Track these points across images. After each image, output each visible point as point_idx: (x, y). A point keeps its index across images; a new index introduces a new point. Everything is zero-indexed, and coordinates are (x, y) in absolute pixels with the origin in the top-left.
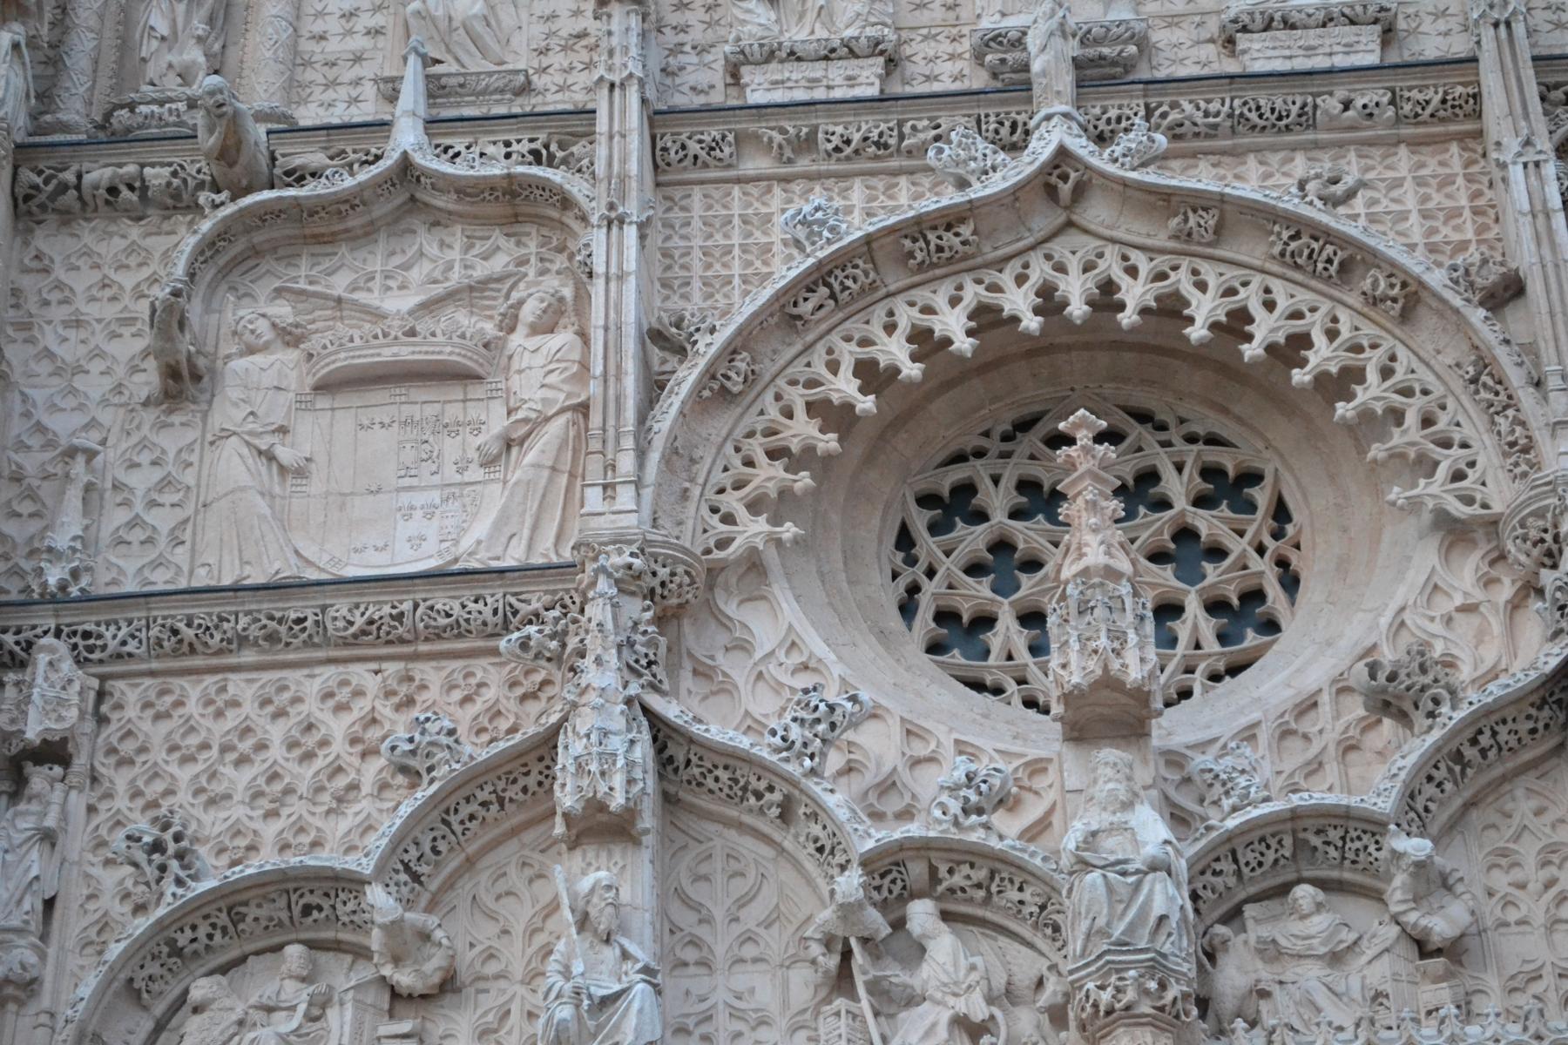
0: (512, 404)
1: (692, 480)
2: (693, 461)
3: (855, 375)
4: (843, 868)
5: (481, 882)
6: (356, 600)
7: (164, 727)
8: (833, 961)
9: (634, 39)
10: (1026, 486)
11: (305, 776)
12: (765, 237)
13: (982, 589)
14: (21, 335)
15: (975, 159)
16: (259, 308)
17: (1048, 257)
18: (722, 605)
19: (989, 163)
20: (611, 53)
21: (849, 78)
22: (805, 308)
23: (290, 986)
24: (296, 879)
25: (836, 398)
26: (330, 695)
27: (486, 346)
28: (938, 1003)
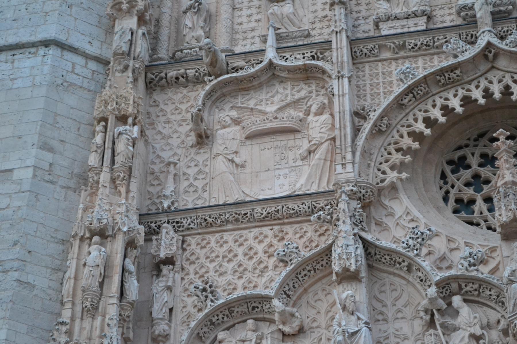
0: (310, 139)
1: (371, 160)
2: (371, 154)
3: (423, 122)
4: (429, 286)
5: (310, 297)
6: (263, 206)
7: (204, 251)
8: (428, 317)
9: (343, 17)
10: (483, 156)
11: (250, 265)
12: (390, 79)
13: (470, 192)
14: (151, 127)
15: (459, 48)
16: (226, 113)
17: (486, 79)
18: (383, 201)
19: (464, 49)
20: (336, 22)
21: (415, 24)
22: (405, 101)
23: (250, 333)
24: (249, 298)
25: (417, 130)
26: (257, 238)
27: (300, 121)
28: (465, 330)
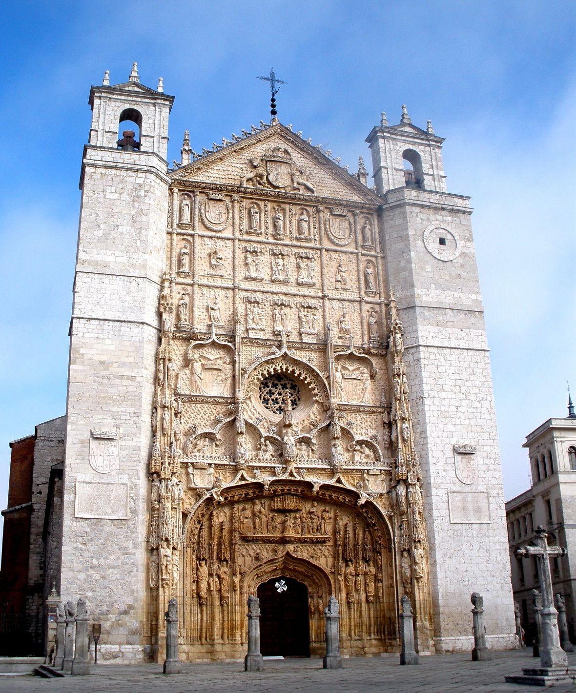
10: (273, 383)
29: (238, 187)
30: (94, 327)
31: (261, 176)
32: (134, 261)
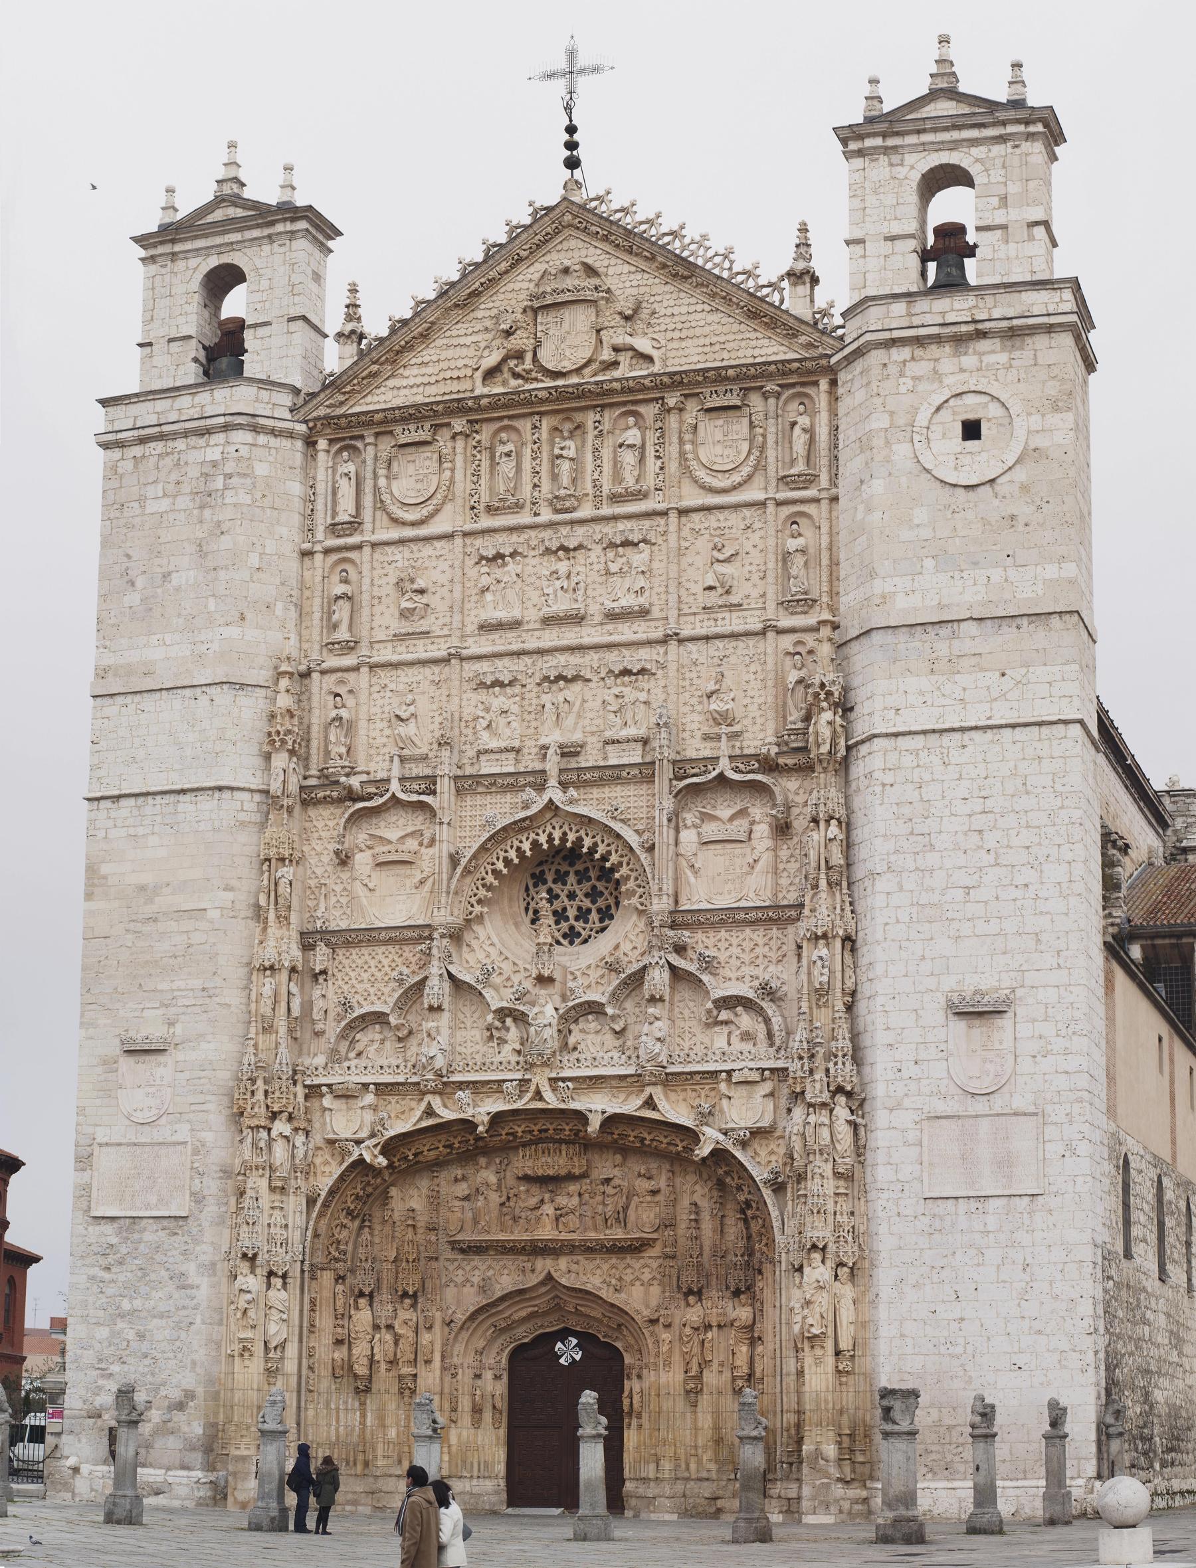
29: (459, 400)
30: (124, 812)
31: (519, 355)
32: (203, 648)
